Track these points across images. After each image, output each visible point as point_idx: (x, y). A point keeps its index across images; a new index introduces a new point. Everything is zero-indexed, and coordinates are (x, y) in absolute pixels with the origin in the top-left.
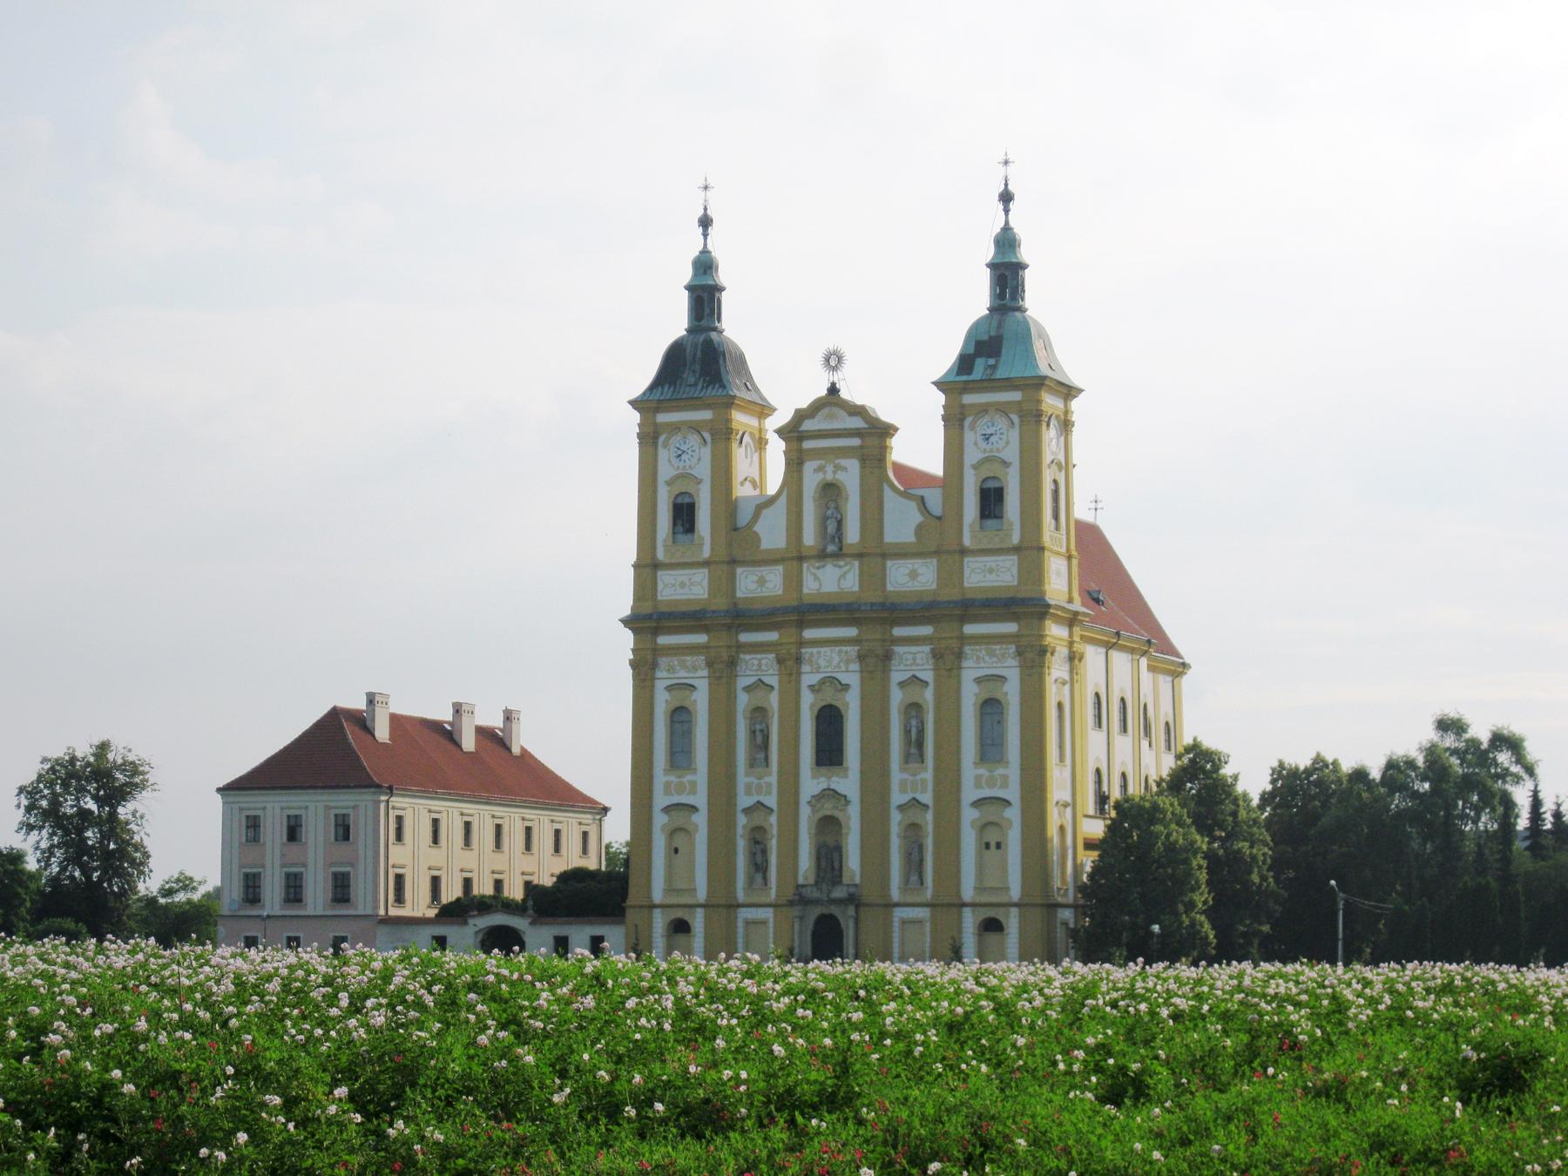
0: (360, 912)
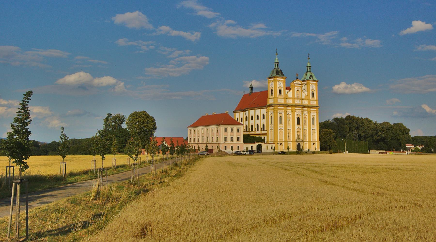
0: (241, 143)
